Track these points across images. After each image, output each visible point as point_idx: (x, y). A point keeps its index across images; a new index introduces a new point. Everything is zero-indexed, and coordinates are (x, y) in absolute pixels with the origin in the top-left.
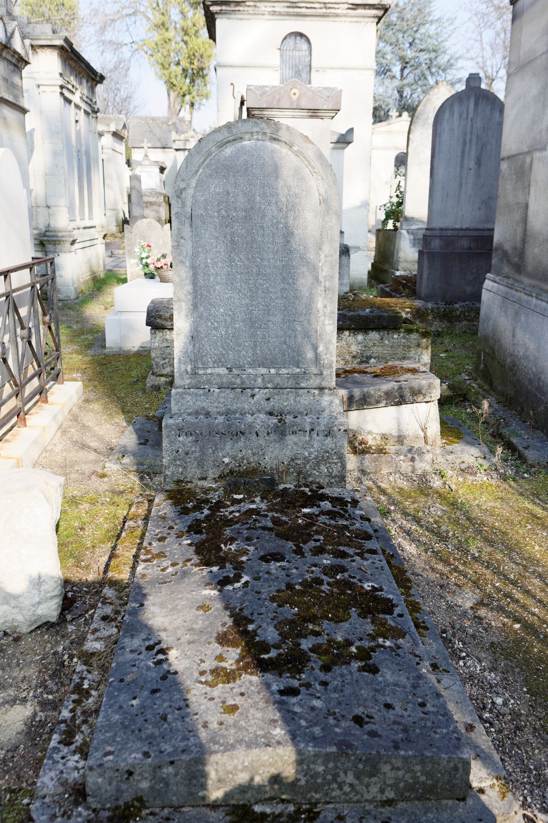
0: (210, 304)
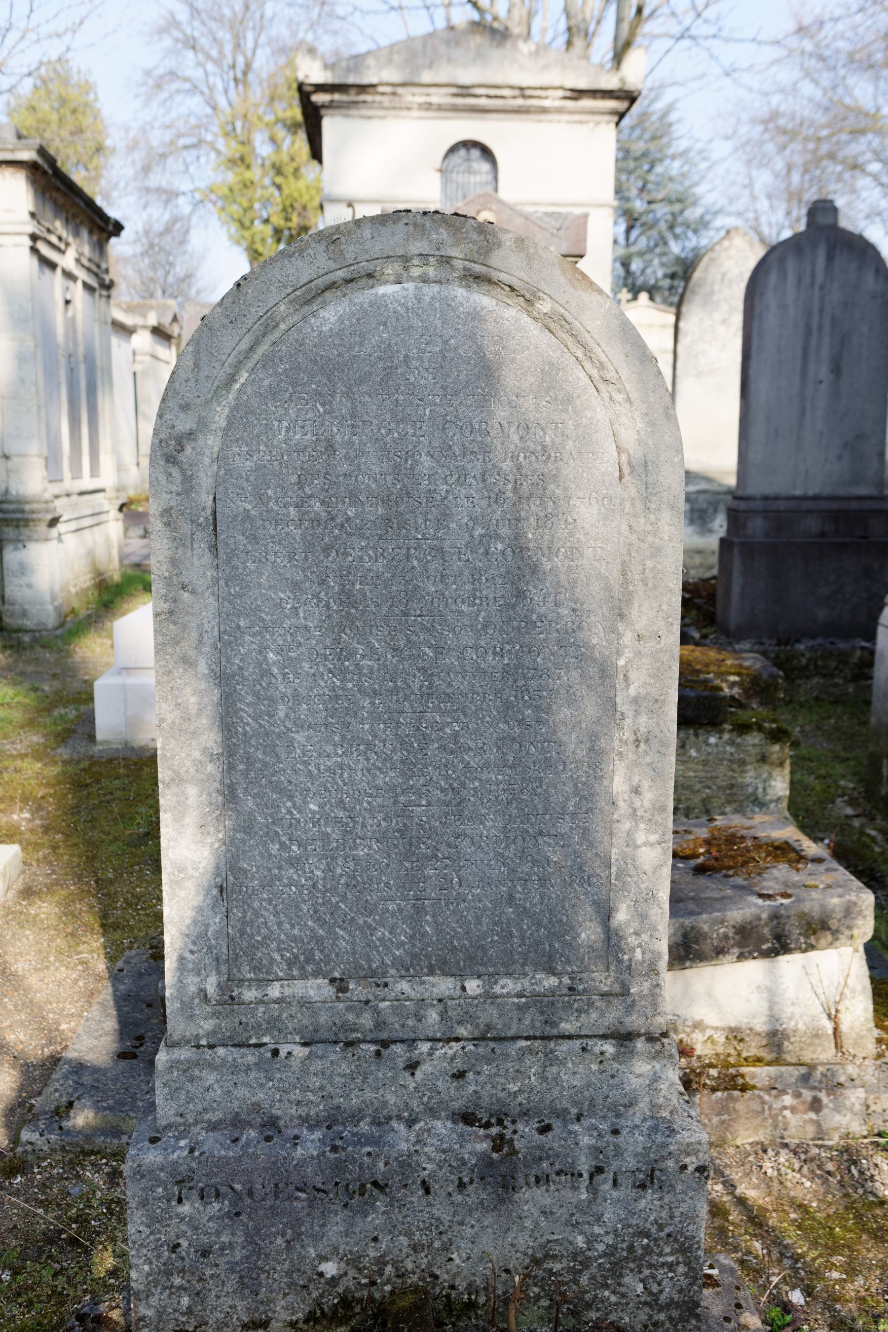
0: (277, 788)
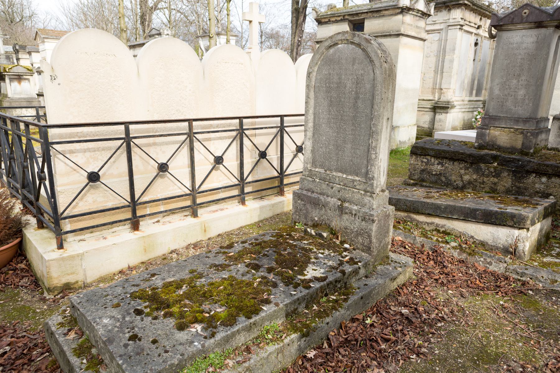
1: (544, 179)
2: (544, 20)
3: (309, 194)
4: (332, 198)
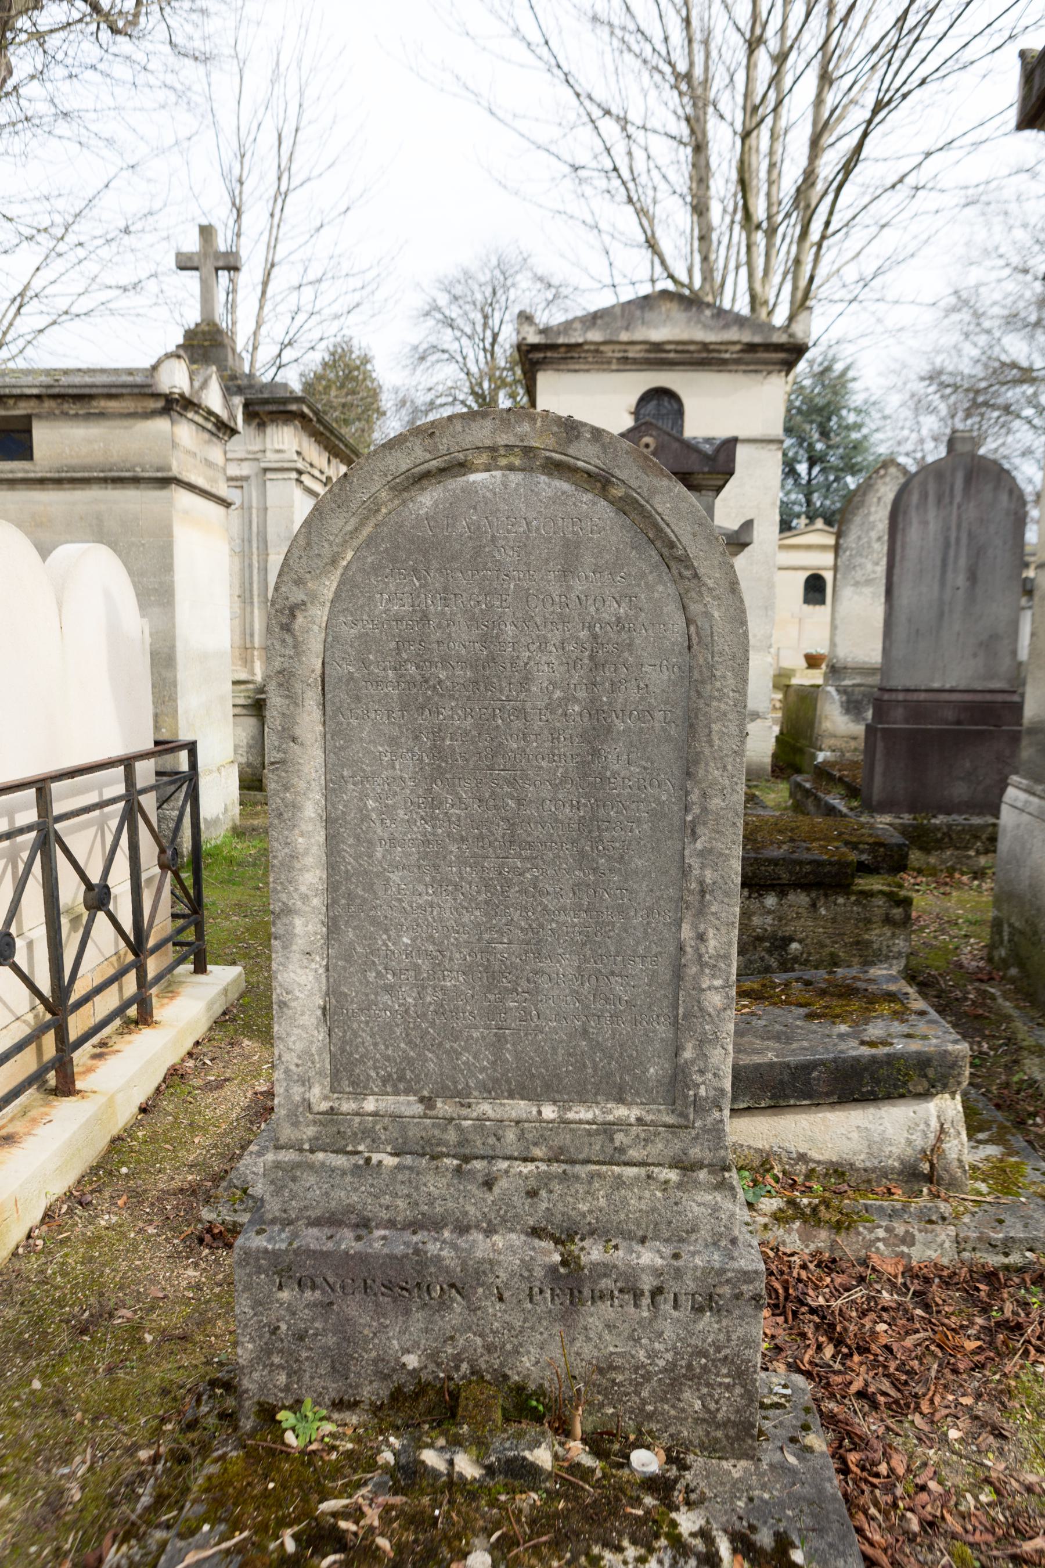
0: (374, 922)
1: (771, 901)
2: (696, 468)
3: (347, 1241)
4: (489, 1232)
